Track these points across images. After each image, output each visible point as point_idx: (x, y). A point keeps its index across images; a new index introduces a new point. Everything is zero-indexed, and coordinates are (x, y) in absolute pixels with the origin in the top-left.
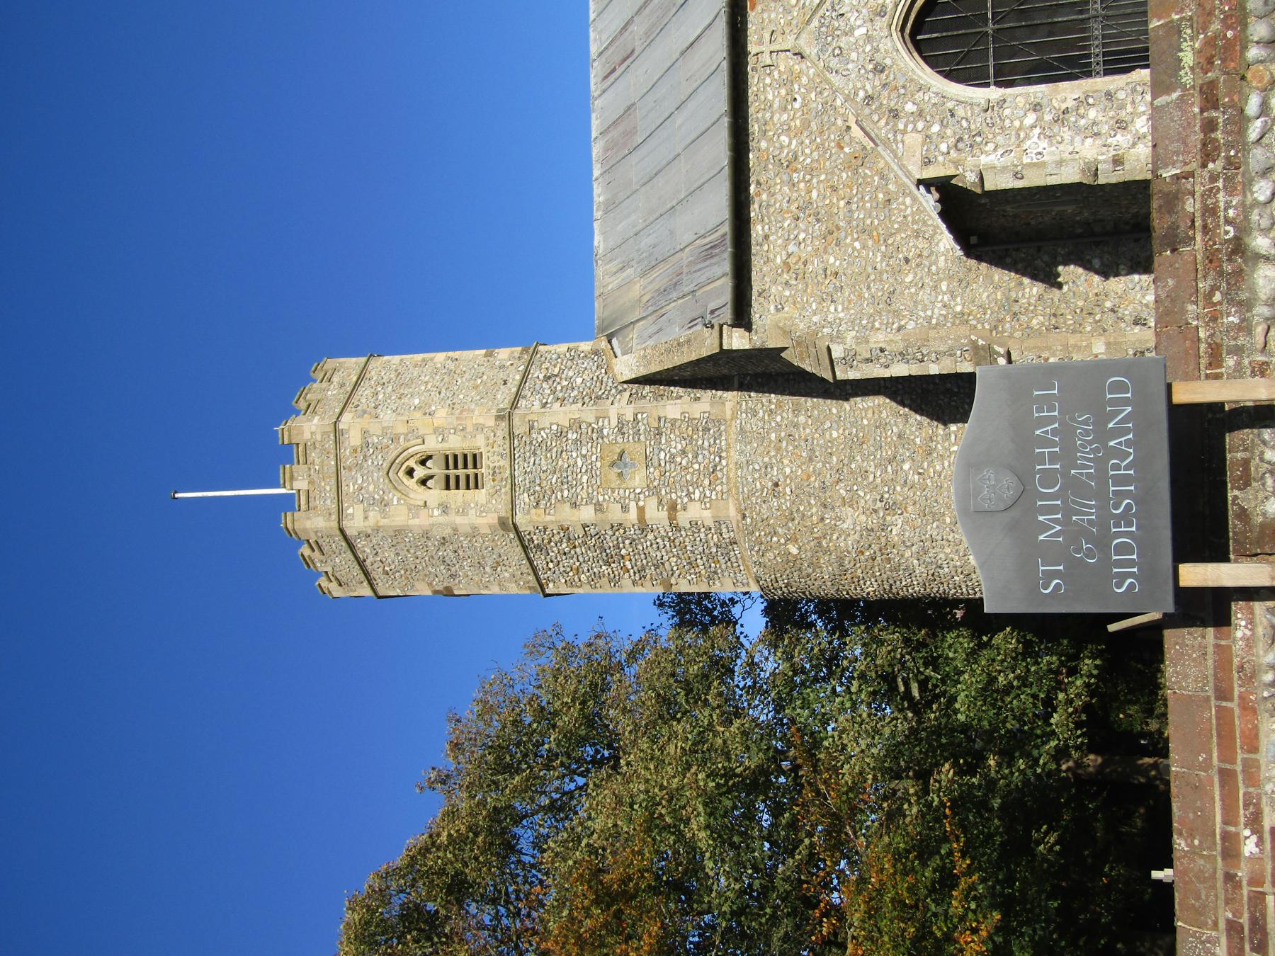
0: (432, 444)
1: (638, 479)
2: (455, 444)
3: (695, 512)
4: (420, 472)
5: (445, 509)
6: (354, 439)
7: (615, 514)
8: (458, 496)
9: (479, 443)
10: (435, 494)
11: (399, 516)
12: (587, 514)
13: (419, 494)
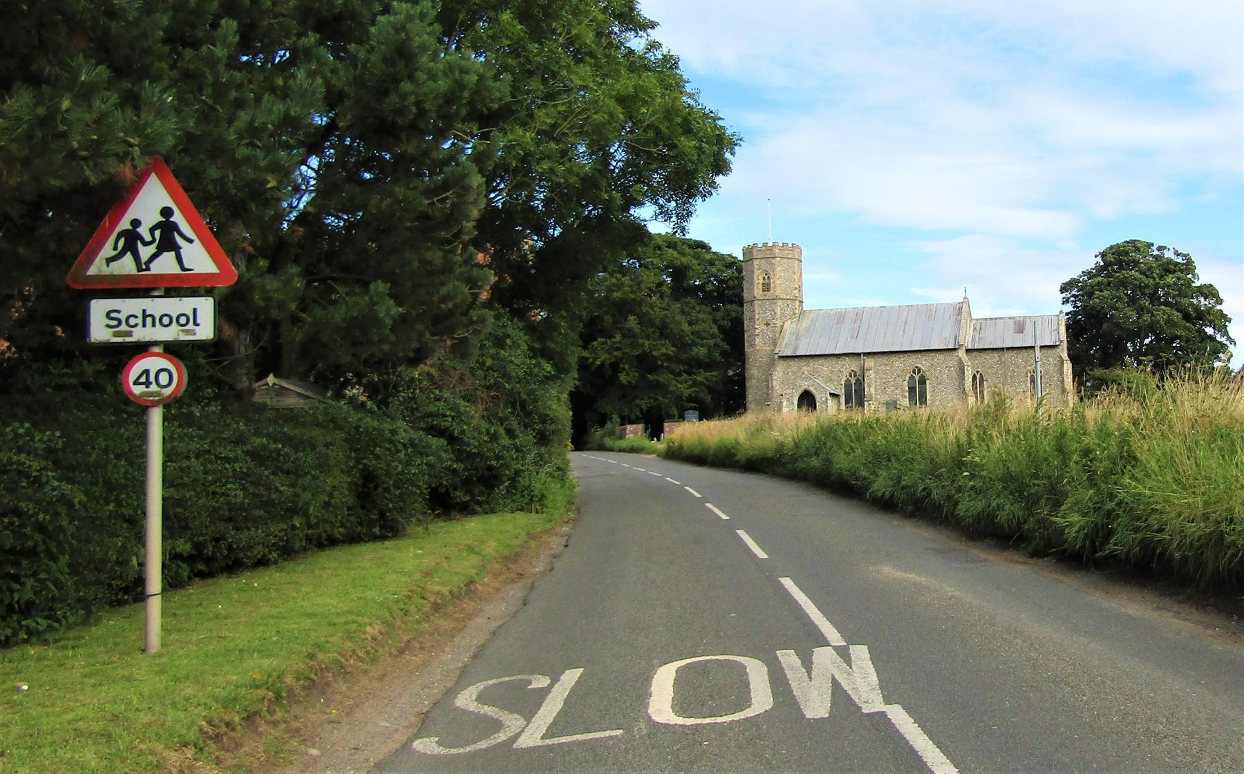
0: (772, 281)
1: (764, 327)
2: (772, 286)
3: (757, 340)
4: (766, 277)
5: (758, 284)
6: (773, 261)
7: (757, 323)
8: (760, 287)
9: (772, 292)
10: (761, 281)
11: (757, 272)
12: (757, 317)
13: (761, 278)
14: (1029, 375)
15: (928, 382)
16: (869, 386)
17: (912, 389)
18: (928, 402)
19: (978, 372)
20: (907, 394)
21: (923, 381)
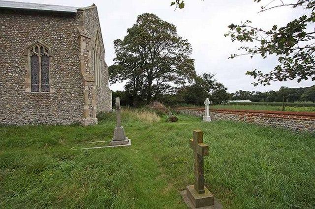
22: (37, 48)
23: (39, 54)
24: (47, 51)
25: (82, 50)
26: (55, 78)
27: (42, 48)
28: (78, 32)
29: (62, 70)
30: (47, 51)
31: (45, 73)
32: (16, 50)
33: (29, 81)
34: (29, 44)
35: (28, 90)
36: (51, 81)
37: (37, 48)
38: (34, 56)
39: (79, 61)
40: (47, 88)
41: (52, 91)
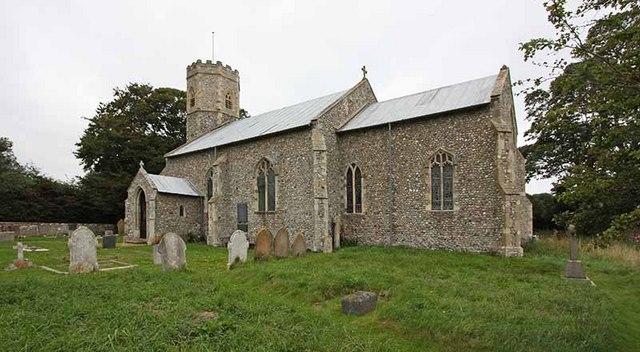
14: (430, 166)
15: (276, 178)
16: (216, 186)
17: (261, 188)
18: (277, 206)
19: (353, 165)
20: (256, 195)
21: (272, 174)
22: (438, 156)
23: (441, 164)
24: (450, 159)
25: (500, 152)
26: (460, 192)
27: (444, 156)
28: (493, 127)
29: (470, 180)
30: (450, 159)
31: (448, 185)
32: (416, 162)
33: (429, 196)
34: (431, 153)
35: (429, 208)
36: (455, 196)
37: (438, 156)
38: (436, 167)
39: (494, 166)
40: (450, 205)
41: (456, 208)
